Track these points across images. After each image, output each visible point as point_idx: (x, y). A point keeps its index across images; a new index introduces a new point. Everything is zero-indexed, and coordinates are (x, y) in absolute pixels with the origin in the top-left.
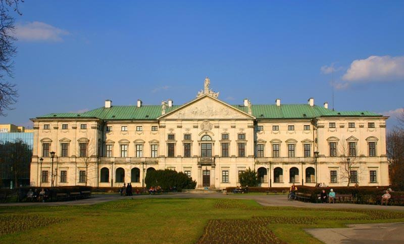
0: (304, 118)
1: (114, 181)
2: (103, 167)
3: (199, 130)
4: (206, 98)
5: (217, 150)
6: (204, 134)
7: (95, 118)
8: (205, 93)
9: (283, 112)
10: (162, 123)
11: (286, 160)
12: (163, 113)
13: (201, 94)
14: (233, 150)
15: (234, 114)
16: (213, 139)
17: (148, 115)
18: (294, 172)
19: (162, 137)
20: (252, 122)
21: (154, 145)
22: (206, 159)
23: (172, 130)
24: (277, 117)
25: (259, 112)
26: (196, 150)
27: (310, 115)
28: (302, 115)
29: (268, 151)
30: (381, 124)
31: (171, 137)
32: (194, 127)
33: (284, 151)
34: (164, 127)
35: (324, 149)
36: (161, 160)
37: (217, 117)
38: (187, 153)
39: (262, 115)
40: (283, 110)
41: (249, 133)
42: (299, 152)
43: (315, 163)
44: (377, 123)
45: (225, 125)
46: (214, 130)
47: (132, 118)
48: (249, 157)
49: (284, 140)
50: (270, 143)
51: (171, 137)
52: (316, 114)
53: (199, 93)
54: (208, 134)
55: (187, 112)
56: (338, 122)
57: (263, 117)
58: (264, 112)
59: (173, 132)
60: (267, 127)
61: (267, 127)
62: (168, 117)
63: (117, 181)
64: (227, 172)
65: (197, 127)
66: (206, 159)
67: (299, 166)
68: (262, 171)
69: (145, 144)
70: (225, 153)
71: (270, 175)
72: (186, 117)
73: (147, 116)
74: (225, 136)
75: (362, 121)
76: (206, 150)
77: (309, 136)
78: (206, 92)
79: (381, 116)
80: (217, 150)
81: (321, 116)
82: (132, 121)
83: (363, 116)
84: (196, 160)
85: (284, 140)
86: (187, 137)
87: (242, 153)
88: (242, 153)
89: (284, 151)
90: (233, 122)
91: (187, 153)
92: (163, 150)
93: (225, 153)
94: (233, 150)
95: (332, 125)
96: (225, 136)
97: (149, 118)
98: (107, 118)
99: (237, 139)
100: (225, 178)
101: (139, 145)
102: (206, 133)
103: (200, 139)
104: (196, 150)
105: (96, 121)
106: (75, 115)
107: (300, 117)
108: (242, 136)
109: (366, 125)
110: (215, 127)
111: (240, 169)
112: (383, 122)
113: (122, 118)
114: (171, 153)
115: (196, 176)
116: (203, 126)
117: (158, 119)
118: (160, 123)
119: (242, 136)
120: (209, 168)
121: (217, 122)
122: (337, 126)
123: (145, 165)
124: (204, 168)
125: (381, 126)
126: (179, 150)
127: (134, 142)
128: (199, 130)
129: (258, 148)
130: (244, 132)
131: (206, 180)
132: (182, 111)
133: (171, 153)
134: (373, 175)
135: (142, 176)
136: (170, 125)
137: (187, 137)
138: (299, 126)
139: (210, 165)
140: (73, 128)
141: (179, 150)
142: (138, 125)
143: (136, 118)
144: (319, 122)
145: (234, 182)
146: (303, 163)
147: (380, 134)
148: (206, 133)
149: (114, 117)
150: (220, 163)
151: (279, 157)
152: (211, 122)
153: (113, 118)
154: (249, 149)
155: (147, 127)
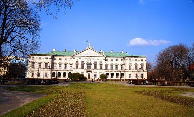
0: (121, 57)
1: (57, 77)
3: (87, 60)
4: (89, 49)
5: (93, 67)
6: (89, 61)
7: (51, 55)
10: (74, 57)
11: (115, 70)
12: (75, 54)
13: (88, 48)
14: (98, 67)
15: (98, 55)
18: (118, 74)
19: (74, 61)
20: (105, 58)
21: (71, 65)
22: (89, 70)
23: (77, 60)
24: (112, 56)
26: (86, 67)
27: (122, 56)
29: (109, 67)
31: (77, 62)
33: (114, 67)
34: (75, 59)
35: (128, 67)
36: (74, 70)
38: (83, 68)
41: (103, 61)
42: (119, 68)
43: (124, 72)
44: (144, 59)
46: (92, 60)
48: (103, 69)
50: (58, 64)
51: (77, 62)
52: (124, 56)
53: (87, 47)
54: (90, 61)
55: (83, 54)
56: (132, 59)
57: (107, 56)
59: (78, 60)
60: (109, 59)
61: (109, 59)
63: (58, 77)
64: (96, 74)
65: (86, 59)
66: (89, 70)
67: (119, 73)
68: (108, 74)
69: (68, 64)
70: (95, 68)
72: (82, 55)
73: (68, 55)
74: (95, 62)
75: (139, 58)
76: (89, 67)
77: (122, 63)
78: (89, 47)
79: (145, 57)
80: (93, 67)
81: (127, 56)
82: (63, 56)
83: (139, 57)
84: (85, 70)
86: (83, 62)
87: (101, 68)
88: (101, 68)
89: (114, 67)
90: (98, 57)
91: (83, 68)
92: (74, 66)
93: (95, 68)
94: (98, 67)
95: (130, 59)
96: (95, 62)
99: (81, 63)
101: (65, 65)
103: (87, 63)
104: (86, 67)
105: (51, 56)
108: (101, 62)
109: (141, 60)
110: (92, 59)
111: (101, 73)
112: (146, 59)
114: (77, 67)
115: (86, 75)
119: (101, 62)
120: (90, 73)
121: (93, 57)
122: (132, 60)
123: (68, 72)
124: (88, 73)
125: (145, 60)
126: (80, 66)
127: (64, 63)
128: (87, 60)
129: (106, 66)
130: (102, 61)
131: (89, 77)
133: (77, 67)
134: (130, 75)
135: (67, 75)
136: (77, 58)
137: (83, 62)
138: (119, 59)
139: (90, 72)
140: (36, 58)
141: (80, 66)
142: (60, 58)
144: (126, 58)
145: (98, 77)
146: (121, 72)
147: (145, 63)
149: (57, 55)
150: (94, 71)
151: (107, 69)
154: (103, 67)
155: (68, 58)
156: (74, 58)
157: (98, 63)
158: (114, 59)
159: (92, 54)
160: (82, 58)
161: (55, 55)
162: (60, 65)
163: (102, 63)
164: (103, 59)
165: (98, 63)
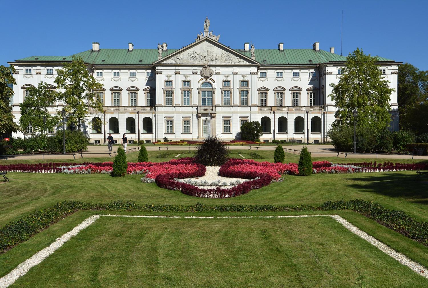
2: (97, 116)
5: (218, 97)
6: (204, 80)
8: (205, 36)
9: (287, 57)
10: (158, 69)
12: (160, 58)
14: (236, 97)
15: (235, 60)
16: (214, 86)
17: (141, 59)
18: (299, 124)
25: (262, 57)
27: (316, 61)
28: (307, 60)
29: (271, 100)
30: (393, 71)
31: (169, 82)
32: (193, 73)
34: (161, 73)
37: (219, 62)
39: (265, 61)
40: (286, 55)
45: (225, 71)
47: (124, 63)
49: (288, 88)
52: (323, 60)
54: (209, 80)
55: (185, 56)
58: (267, 57)
62: (165, 62)
65: (196, 73)
67: (304, 116)
68: (266, 121)
71: (274, 125)
73: (141, 61)
79: (393, 62)
80: (218, 97)
85: (288, 88)
86: (186, 82)
87: (244, 102)
89: (288, 100)
90: (235, 68)
94: (236, 97)
96: (227, 82)
97: (142, 63)
98: (97, 63)
100: (227, 130)
102: (207, 79)
104: (196, 98)
106: (61, 59)
107: (306, 63)
110: (216, 74)
112: (395, 68)
113: (113, 63)
116: (202, 72)
117: (154, 64)
118: (157, 68)
125: (392, 73)
128: (198, 77)
132: (181, 56)
143: (129, 63)
148: (207, 79)
149: (103, 61)
150: (221, 112)
152: (211, 68)
153: (103, 63)
154: (254, 98)
156: (159, 71)
157: (236, 85)
158: (288, 73)
159: (214, 55)
160: (184, 71)
161: (99, 61)
162: (117, 92)
163: (250, 87)
164: (252, 74)
165: (236, 85)
